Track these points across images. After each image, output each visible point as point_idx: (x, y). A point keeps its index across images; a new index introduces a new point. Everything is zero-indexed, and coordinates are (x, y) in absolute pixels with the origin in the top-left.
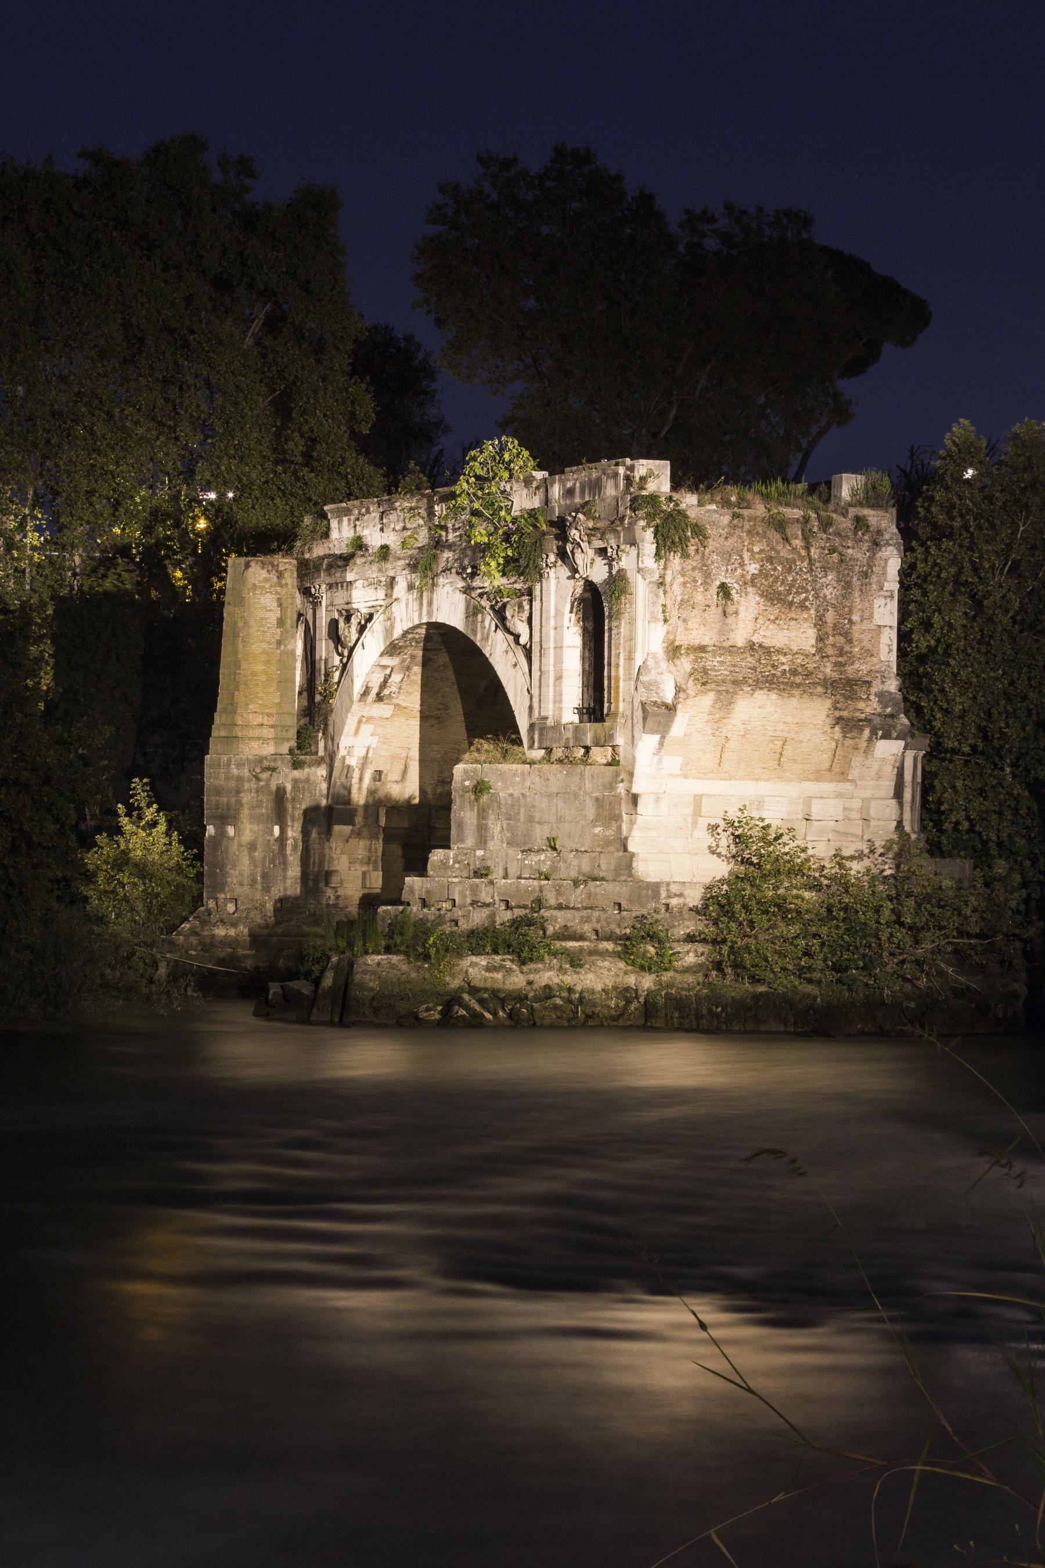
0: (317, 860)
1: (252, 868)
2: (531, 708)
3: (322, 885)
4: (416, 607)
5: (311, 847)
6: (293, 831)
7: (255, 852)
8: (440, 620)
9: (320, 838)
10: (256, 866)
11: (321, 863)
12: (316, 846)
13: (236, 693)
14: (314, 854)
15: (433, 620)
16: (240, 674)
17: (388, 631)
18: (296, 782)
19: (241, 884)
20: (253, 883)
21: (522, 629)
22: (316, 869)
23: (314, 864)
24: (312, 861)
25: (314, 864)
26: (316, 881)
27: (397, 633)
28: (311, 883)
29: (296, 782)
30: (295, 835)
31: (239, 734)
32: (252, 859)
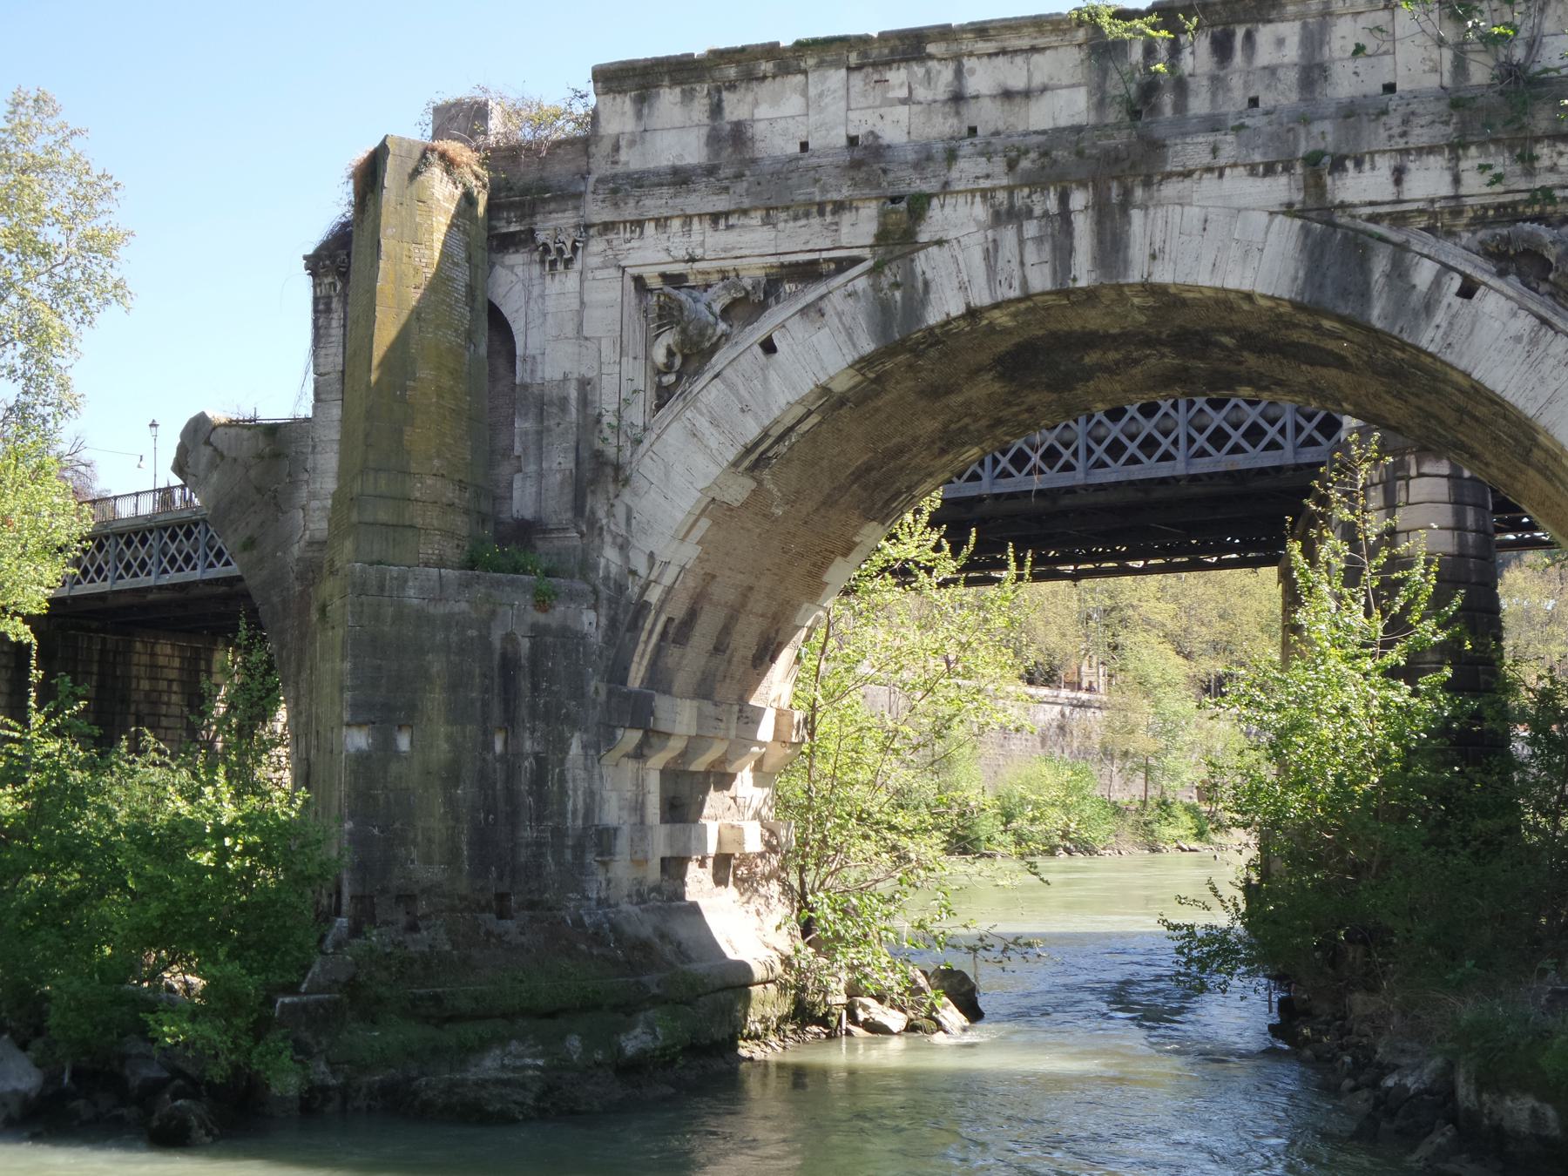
0: (580, 805)
1: (451, 823)
3: (590, 858)
5: (569, 776)
6: (533, 739)
7: (457, 787)
8: (1163, 275)
9: (586, 755)
10: (457, 819)
11: (589, 812)
12: (581, 774)
13: (408, 429)
14: (575, 791)
16: (414, 389)
18: (537, 632)
19: (428, 860)
20: (453, 857)
22: (580, 822)
23: (575, 812)
24: (570, 806)
25: (575, 812)
26: (580, 849)
28: (568, 855)
29: (537, 632)
30: (537, 749)
31: (419, 521)
32: (450, 802)
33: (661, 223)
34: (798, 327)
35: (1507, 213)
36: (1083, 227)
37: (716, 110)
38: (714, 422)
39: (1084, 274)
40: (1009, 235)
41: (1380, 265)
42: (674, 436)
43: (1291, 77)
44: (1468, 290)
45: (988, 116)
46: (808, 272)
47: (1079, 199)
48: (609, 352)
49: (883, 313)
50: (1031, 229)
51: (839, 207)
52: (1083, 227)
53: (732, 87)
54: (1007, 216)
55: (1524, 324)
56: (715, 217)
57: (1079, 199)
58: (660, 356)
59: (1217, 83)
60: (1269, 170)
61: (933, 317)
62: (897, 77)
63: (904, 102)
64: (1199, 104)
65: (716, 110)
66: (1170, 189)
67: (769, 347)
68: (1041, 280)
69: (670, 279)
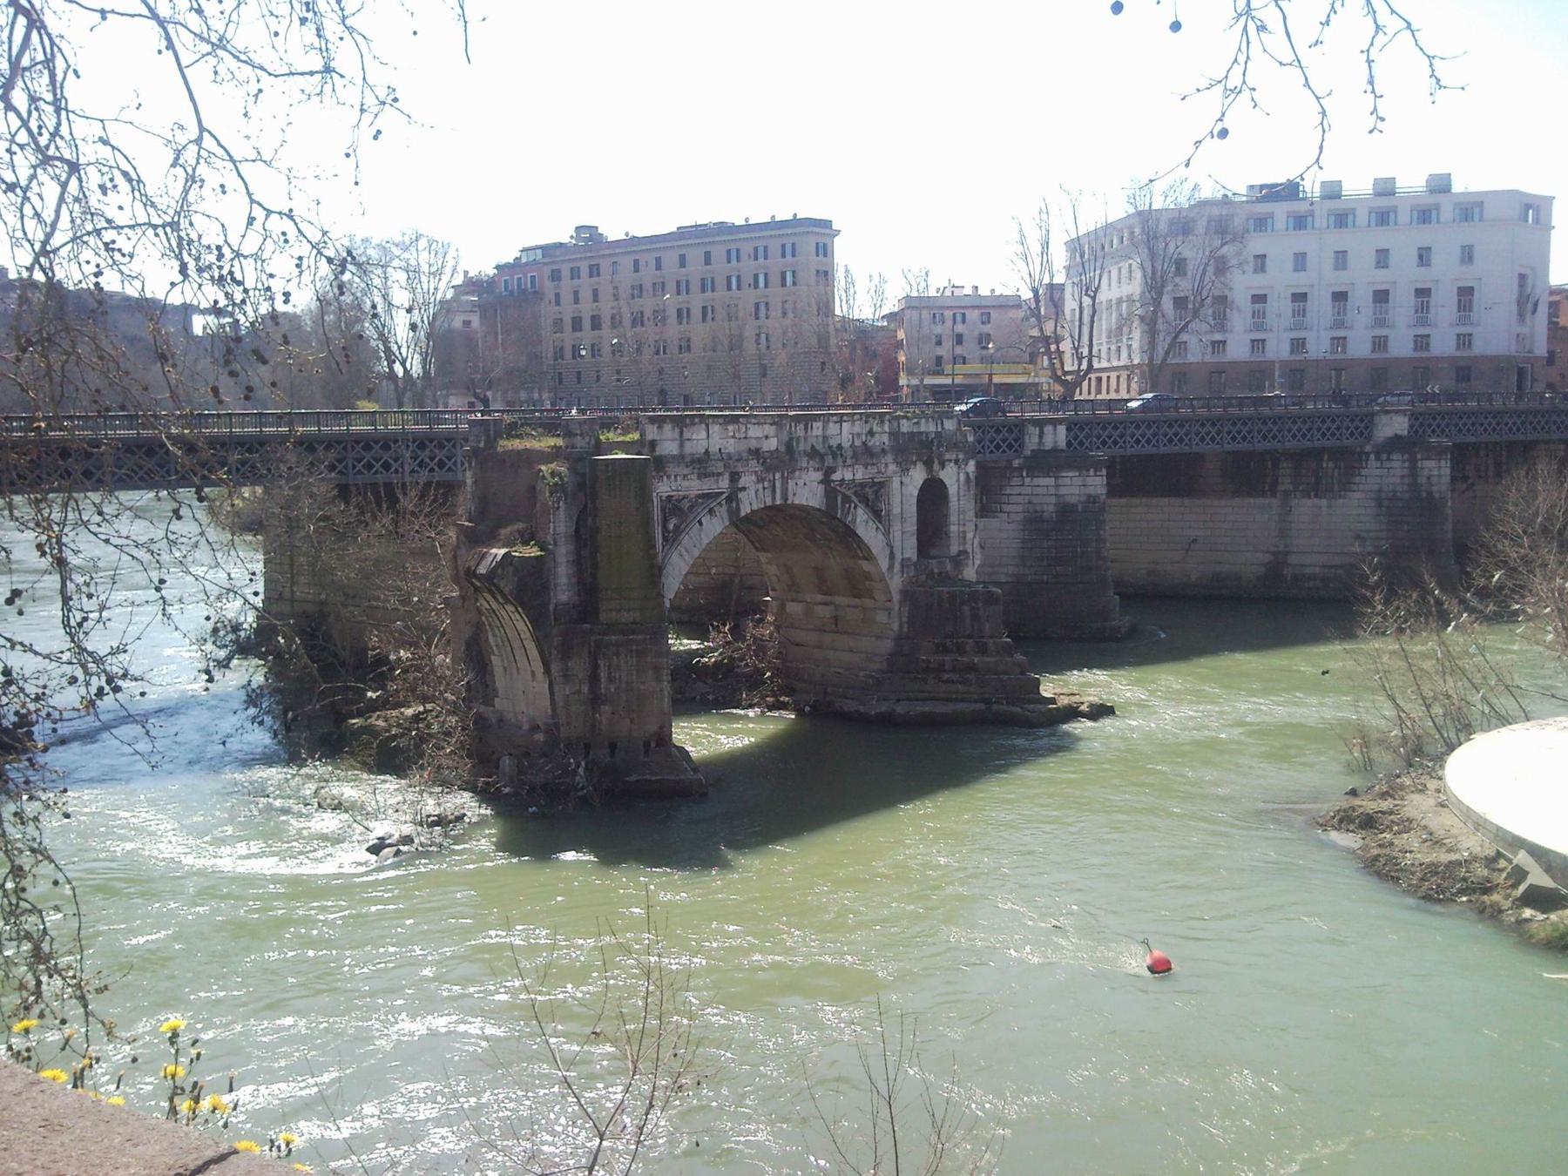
2: (892, 556)
4: (768, 493)
8: (796, 502)
17: (734, 514)
27: (745, 510)
33: (669, 477)
35: (863, 485)
36: (778, 485)
37: (681, 433)
38: (687, 551)
39: (778, 502)
40: (760, 486)
42: (675, 558)
43: (821, 439)
45: (753, 444)
46: (707, 496)
47: (778, 476)
49: (730, 511)
50: (766, 484)
51: (719, 474)
54: (760, 480)
57: (778, 476)
58: (671, 527)
59: (806, 438)
61: (743, 514)
62: (730, 428)
63: (733, 437)
64: (802, 447)
65: (681, 433)
67: (700, 523)
68: (769, 503)
69: (669, 497)
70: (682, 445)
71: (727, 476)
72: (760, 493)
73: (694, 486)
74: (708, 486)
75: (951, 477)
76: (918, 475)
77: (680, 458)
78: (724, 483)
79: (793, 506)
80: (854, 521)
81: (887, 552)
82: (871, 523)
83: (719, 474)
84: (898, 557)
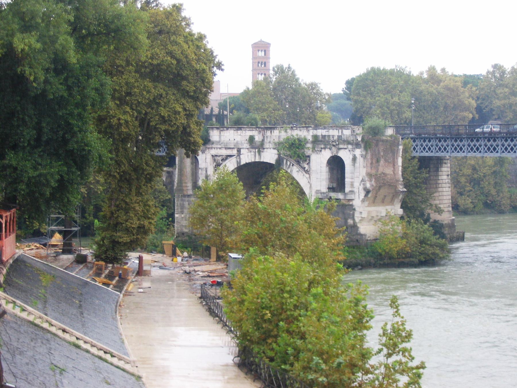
2: (311, 187)
4: (253, 156)
8: (265, 161)
15: (262, 161)
17: (238, 163)
21: (306, 166)
27: (243, 162)
33: (214, 148)
34: (229, 163)
39: (257, 160)
40: (250, 154)
41: (285, 161)
43: (277, 137)
44: (293, 165)
46: (231, 156)
48: (209, 165)
50: (252, 153)
52: (257, 154)
53: (222, 131)
55: (298, 170)
56: (220, 148)
60: (275, 149)
62: (239, 132)
64: (269, 140)
66: (265, 150)
68: (253, 160)
70: (220, 138)
71: (236, 149)
72: (250, 157)
73: (224, 152)
74: (229, 152)
75: (345, 155)
76: (327, 154)
77: (219, 142)
78: (235, 152)
79: (263, 163)
80: (291, 171)
81: (309, 186)
82: (300, 172)
83: (233, 148)
84: (314, 189)
